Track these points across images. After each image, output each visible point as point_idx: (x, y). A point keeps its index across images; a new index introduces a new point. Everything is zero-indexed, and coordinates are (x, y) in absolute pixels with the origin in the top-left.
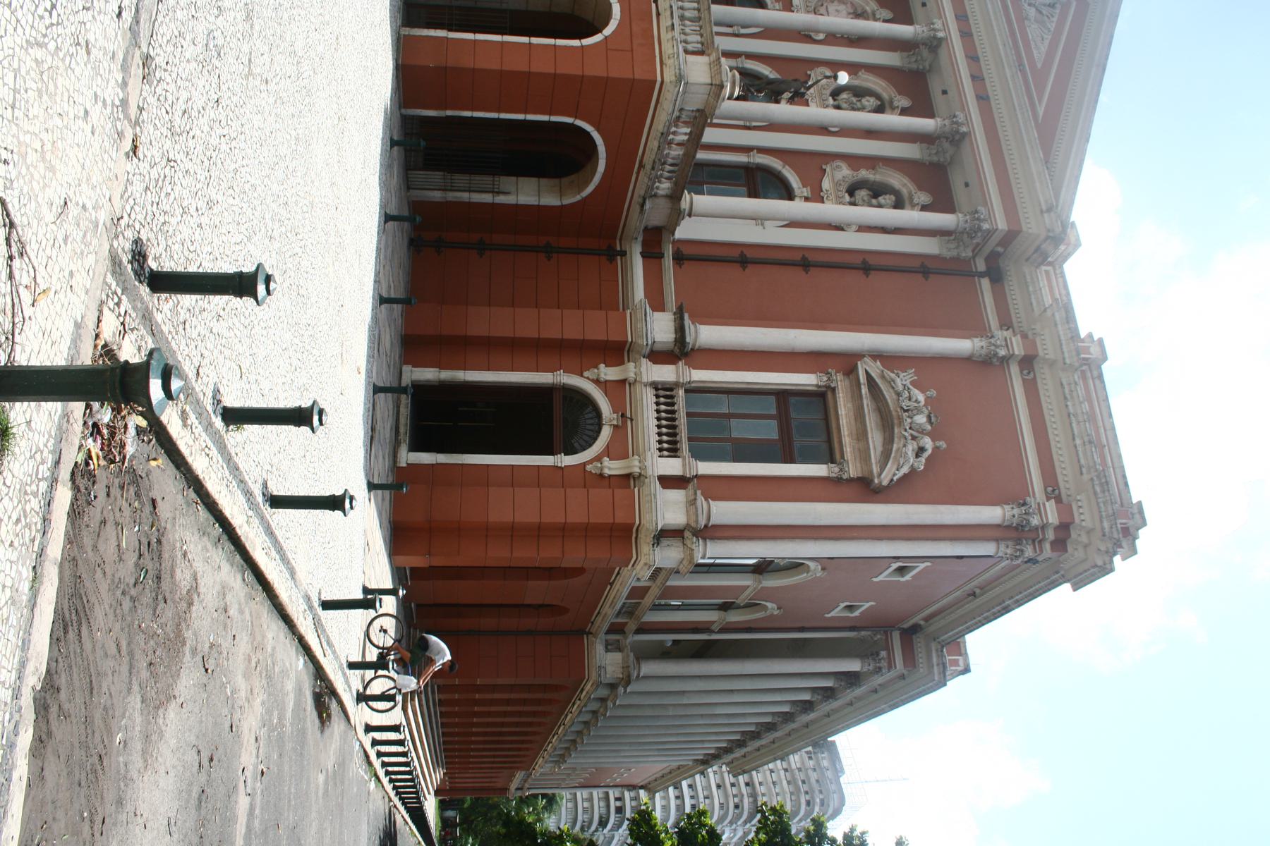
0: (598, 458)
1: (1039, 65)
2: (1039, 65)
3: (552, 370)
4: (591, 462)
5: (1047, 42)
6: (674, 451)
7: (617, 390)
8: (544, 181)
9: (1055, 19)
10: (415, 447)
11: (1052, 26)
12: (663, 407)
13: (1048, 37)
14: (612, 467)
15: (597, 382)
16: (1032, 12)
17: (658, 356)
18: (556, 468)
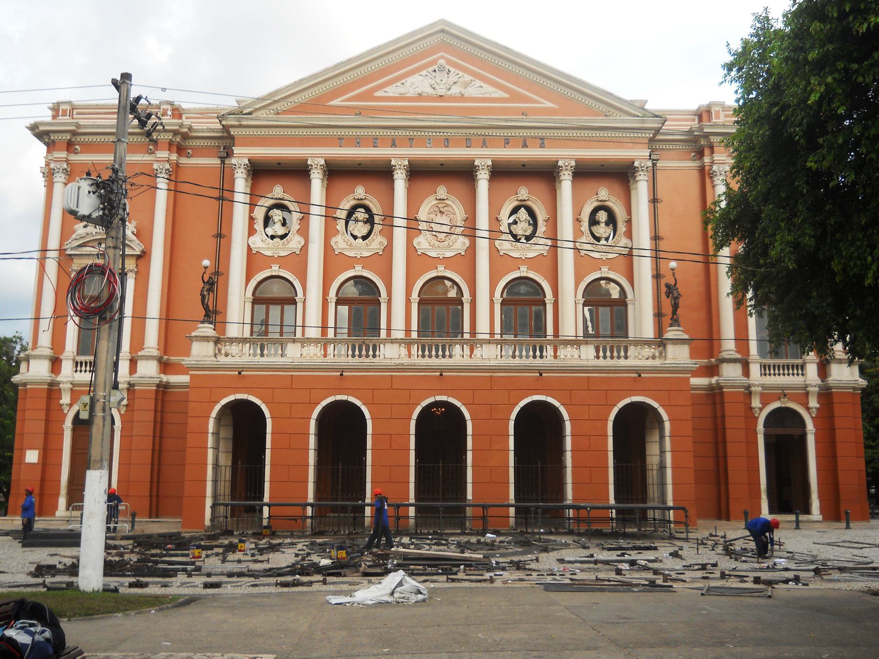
0: (808, 409)
1: (506, 95)
2: (506, 95)
3: (756, 433)
4: (810, 414)
5: (483, 84)
6: (803, 367)
7: (766, 400)
8: (648, 439)
9: (461, 74)
10: (807, 511)
11: (468, 78)
12: (772, 372)
13: (478, 83)
14: (813, 403)
15: (761, 409)
16: (455, 90)
17: (746, 373)
18: (816, 435)
